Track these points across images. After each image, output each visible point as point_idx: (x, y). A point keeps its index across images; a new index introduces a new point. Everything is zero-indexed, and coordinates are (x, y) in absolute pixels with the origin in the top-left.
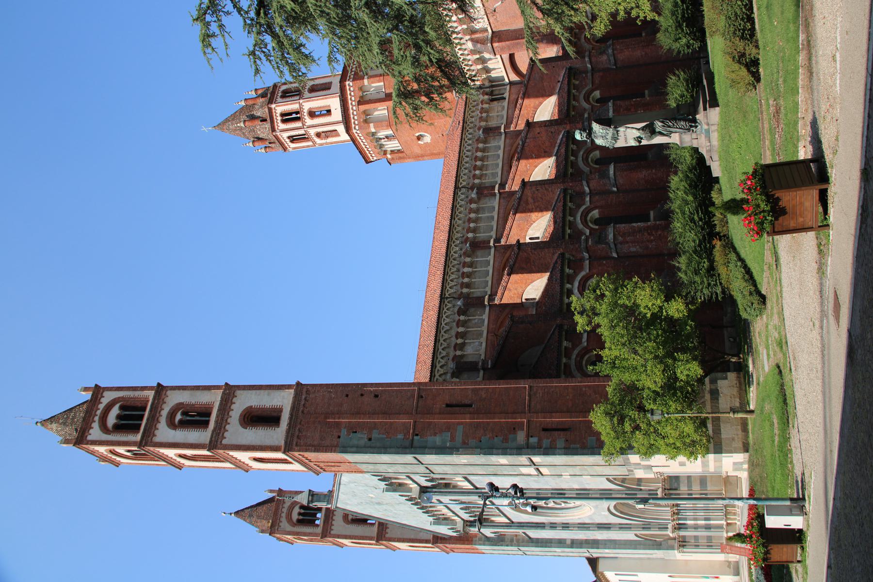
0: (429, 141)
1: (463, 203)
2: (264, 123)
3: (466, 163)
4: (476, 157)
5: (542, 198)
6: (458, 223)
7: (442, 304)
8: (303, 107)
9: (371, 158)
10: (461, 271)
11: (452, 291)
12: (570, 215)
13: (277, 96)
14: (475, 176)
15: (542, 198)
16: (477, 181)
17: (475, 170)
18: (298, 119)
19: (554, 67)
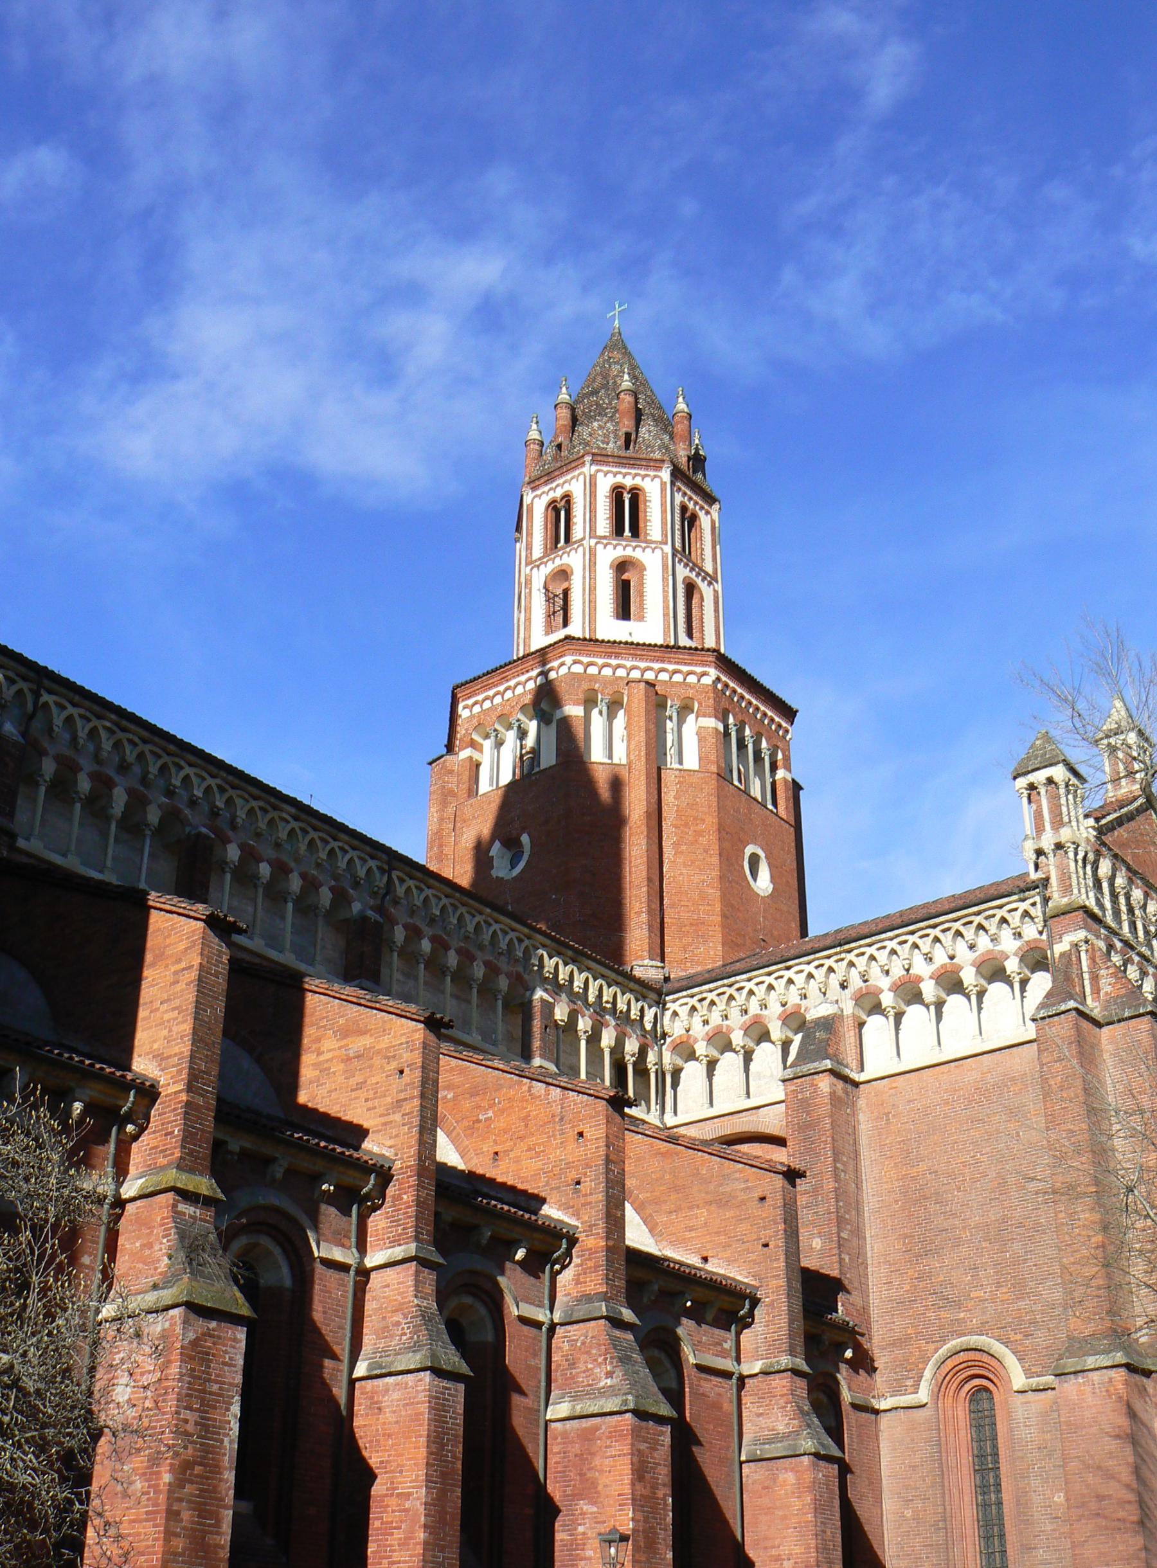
0: (494, 873)
1: (342, 864)
2: (621, 442)
3: (461, 918)
4: (472, 959)
5: (359, 1086)
6: (281, 825)
7: (23, 670)
8: (648, 551)
9: (470, 702)
10: (117, 779)
11: (58, 720)
12: (290, 1172)
13: (690, 499)
14: (414, 933)
15: (359, 1086)
16: (399, 934)
17: (434, 939)
18: (618, 531)
19: (766, 1245)
